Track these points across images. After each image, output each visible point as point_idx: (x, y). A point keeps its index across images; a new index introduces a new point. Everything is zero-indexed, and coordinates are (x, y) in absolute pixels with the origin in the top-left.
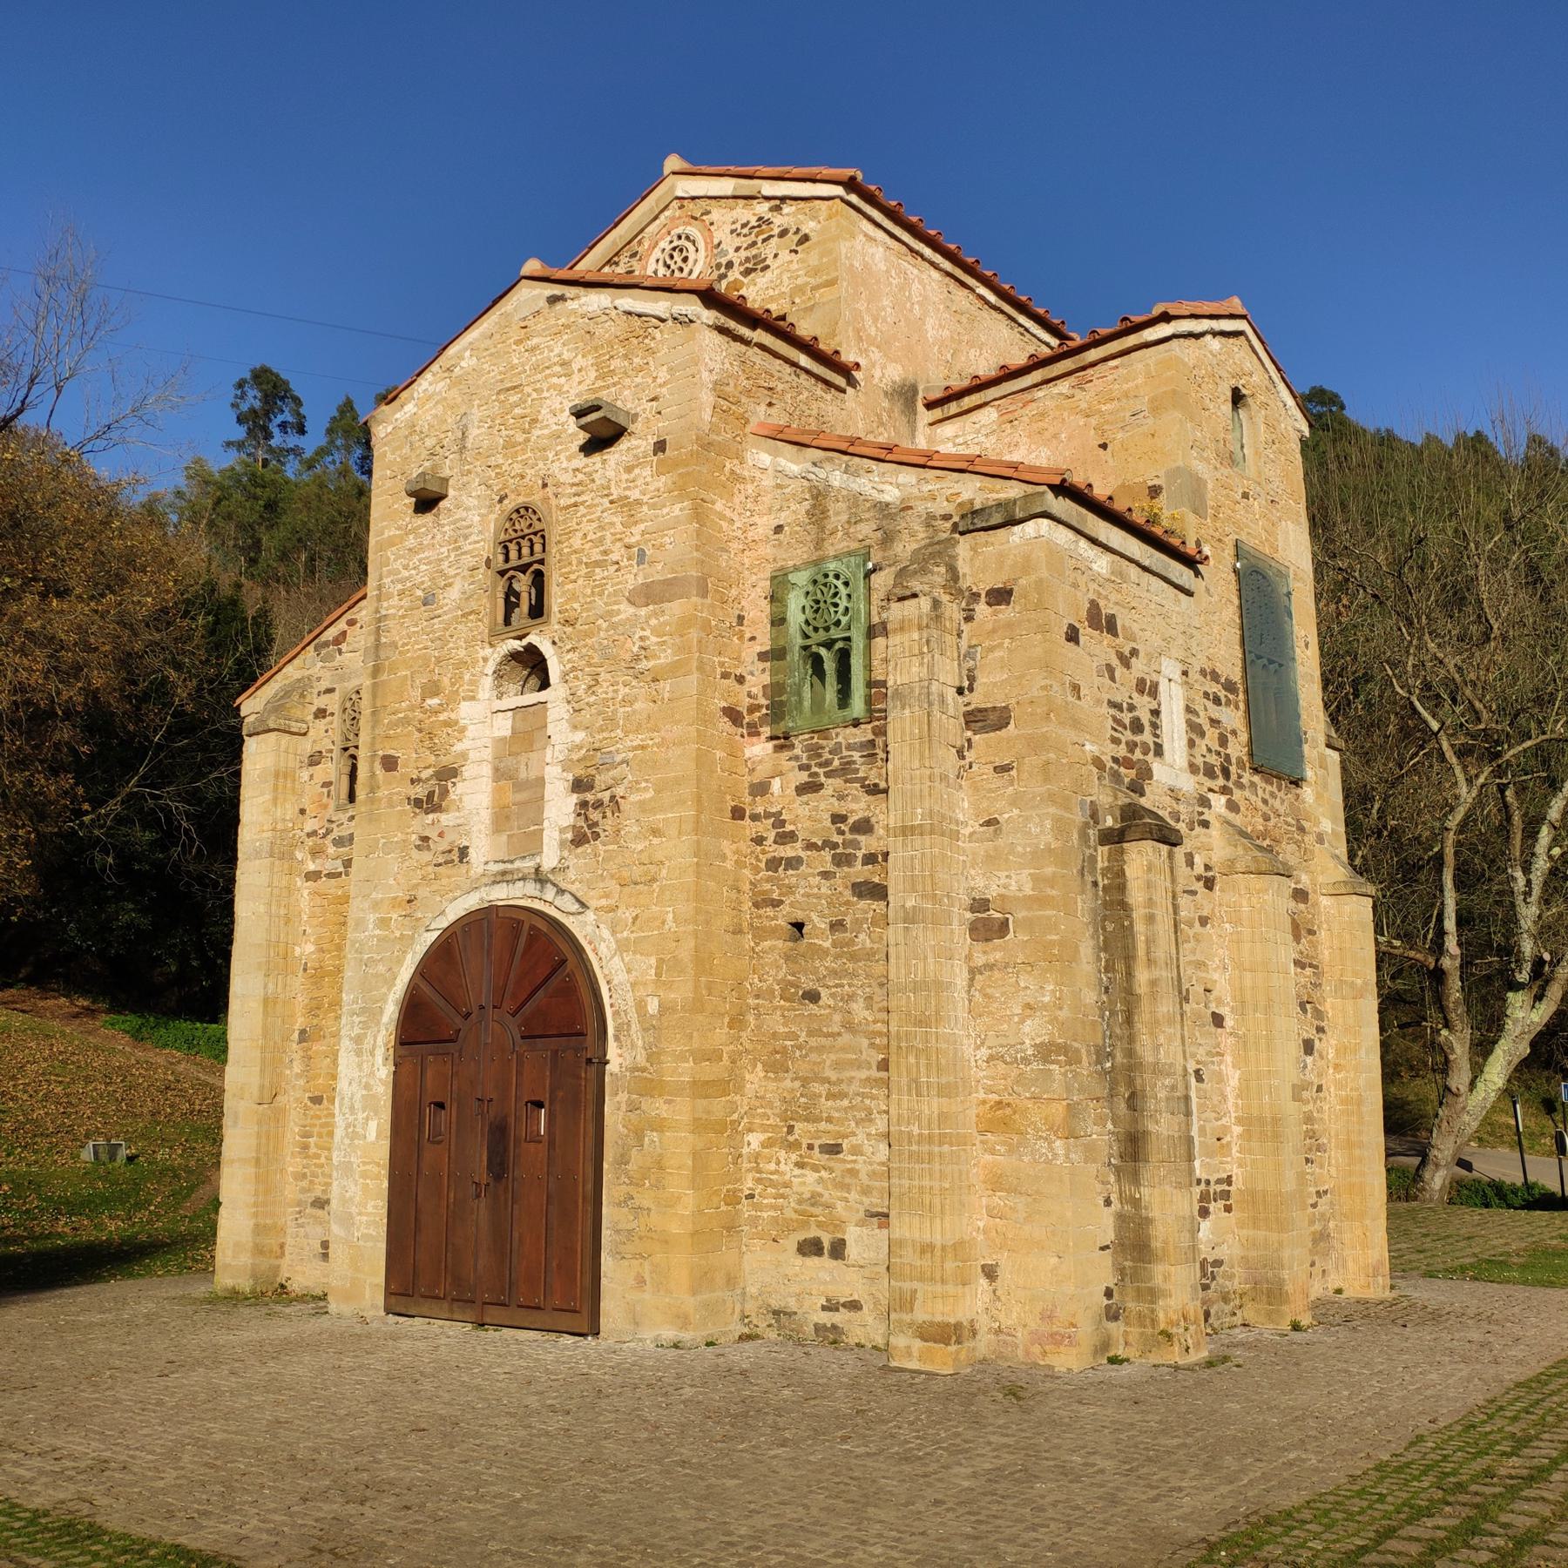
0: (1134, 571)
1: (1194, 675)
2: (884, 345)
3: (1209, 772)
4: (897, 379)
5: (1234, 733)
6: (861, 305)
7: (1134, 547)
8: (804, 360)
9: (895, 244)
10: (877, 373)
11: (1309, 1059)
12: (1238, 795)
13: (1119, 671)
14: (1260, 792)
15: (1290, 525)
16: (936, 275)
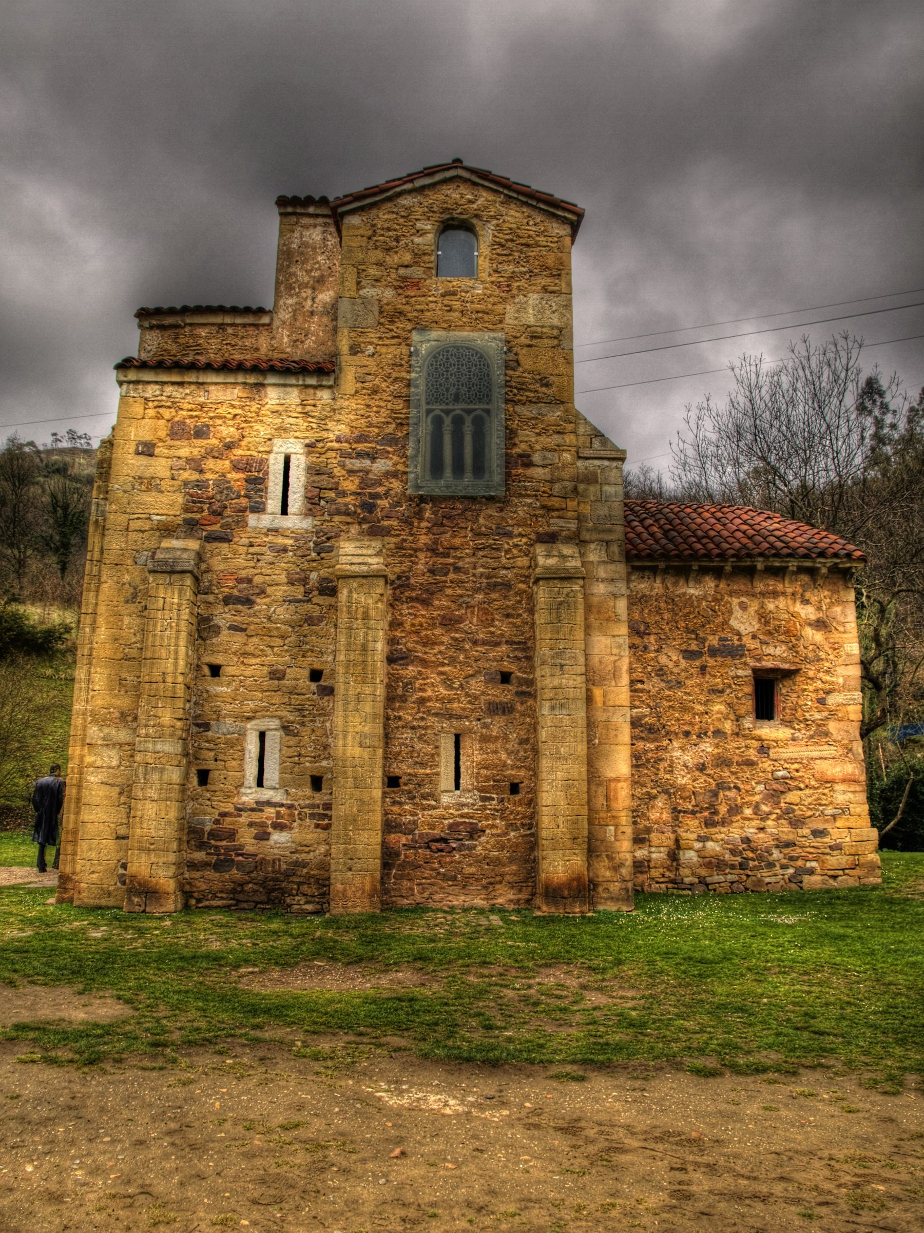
4: (328, 300)
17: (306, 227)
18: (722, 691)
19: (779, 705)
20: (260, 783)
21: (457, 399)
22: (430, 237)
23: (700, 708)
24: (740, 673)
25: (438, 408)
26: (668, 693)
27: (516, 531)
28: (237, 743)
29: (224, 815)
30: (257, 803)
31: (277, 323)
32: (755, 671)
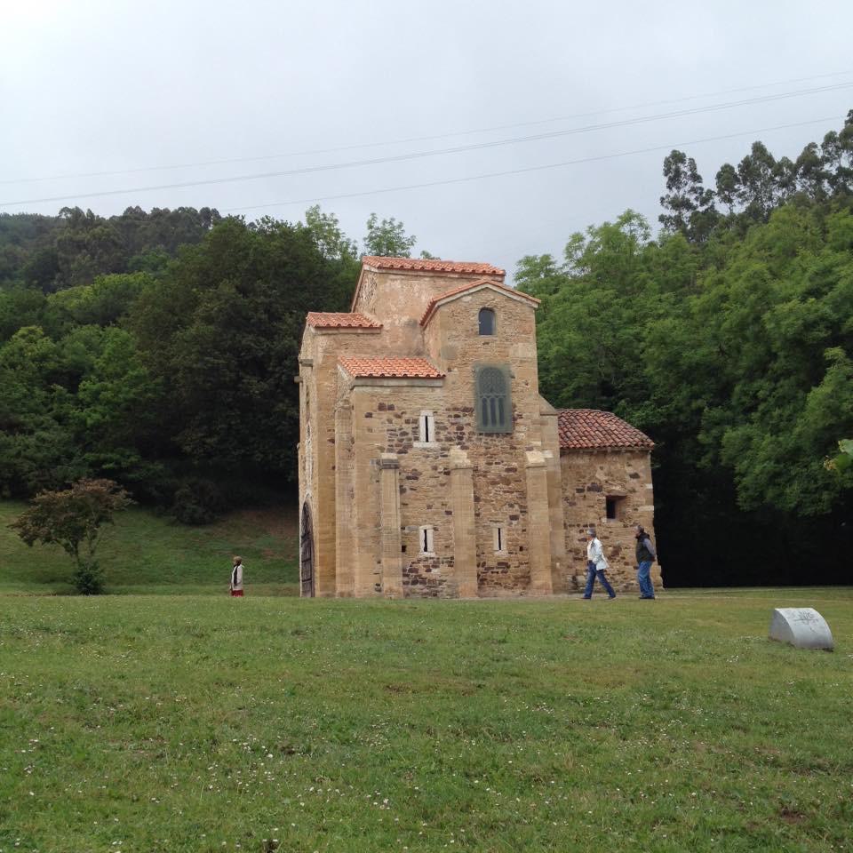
0: (405, 389)
1: (440, 412)
2: (401, 312)
3: (449, 439)
5: (469, 424)
6: (390, 303)
7: (405, 383)
8: (360, 331)
9: (408, 277)
10: (397, 322)
11: (514, 522)
12: (467, 444)
13: (395, 420)
14: (483, 440)
15: (520, 344)
16: (427, 279)
17: (392, 280)
18: (593, 507)
19: (617, 513)
20: (426, 549)
21: (491, 391)
22: (477, 317)
23: (584, 514)
24: (601, 498)
25: (485, 395)
26: (570, 508)
27: (518, 446)
28: (417, 535)
29: (413, 563)
30: (427, 558)
31: (384, 333)
32: (607, 497)
